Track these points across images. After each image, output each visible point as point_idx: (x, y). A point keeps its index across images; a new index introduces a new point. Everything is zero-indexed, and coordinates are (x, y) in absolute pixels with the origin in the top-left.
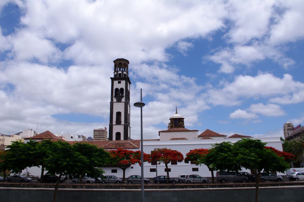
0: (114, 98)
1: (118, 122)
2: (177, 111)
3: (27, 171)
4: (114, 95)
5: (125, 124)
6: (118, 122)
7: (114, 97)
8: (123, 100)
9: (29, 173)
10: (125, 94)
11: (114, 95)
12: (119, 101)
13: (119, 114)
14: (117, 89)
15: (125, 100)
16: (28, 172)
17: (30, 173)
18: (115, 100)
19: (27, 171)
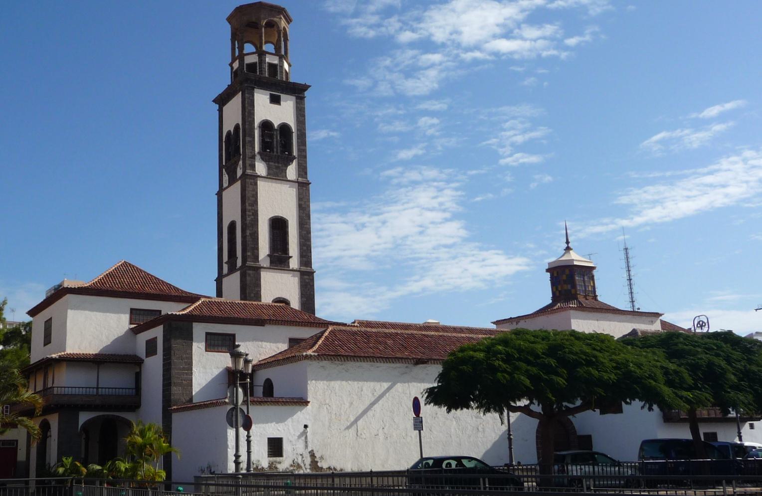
0: (258, 157)
1: (279, 259)
2: (568, 242)
3: (306, 447)
4: (257, 149)
5: (304, 269)
6: (279, 259)
7: (258, 153)
8: (292, 171)
9: (318, 455)
10: (299, 150)
11: (257, 149)
12: (277, 174)
13: (278, 225)
14: (266, 126)
15: (300, 175)
16: (312, 455)
17: (322, 458)
18: (261, 168)
19: (306, 447)
